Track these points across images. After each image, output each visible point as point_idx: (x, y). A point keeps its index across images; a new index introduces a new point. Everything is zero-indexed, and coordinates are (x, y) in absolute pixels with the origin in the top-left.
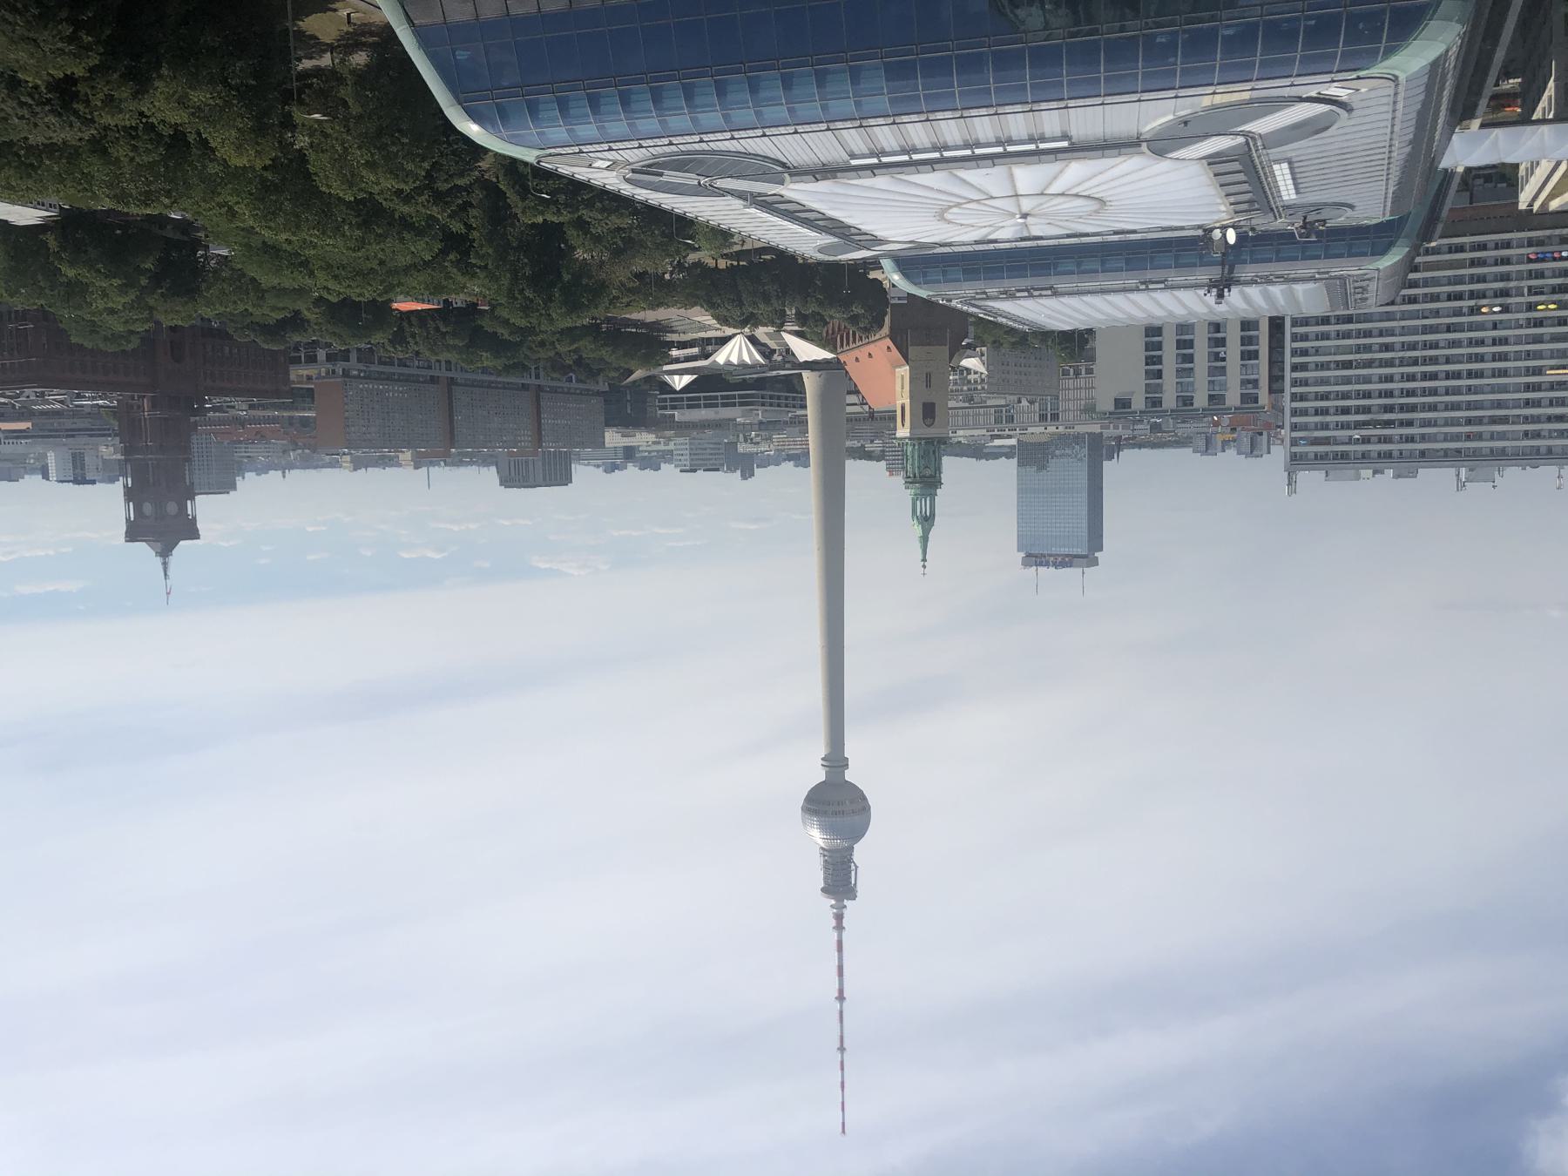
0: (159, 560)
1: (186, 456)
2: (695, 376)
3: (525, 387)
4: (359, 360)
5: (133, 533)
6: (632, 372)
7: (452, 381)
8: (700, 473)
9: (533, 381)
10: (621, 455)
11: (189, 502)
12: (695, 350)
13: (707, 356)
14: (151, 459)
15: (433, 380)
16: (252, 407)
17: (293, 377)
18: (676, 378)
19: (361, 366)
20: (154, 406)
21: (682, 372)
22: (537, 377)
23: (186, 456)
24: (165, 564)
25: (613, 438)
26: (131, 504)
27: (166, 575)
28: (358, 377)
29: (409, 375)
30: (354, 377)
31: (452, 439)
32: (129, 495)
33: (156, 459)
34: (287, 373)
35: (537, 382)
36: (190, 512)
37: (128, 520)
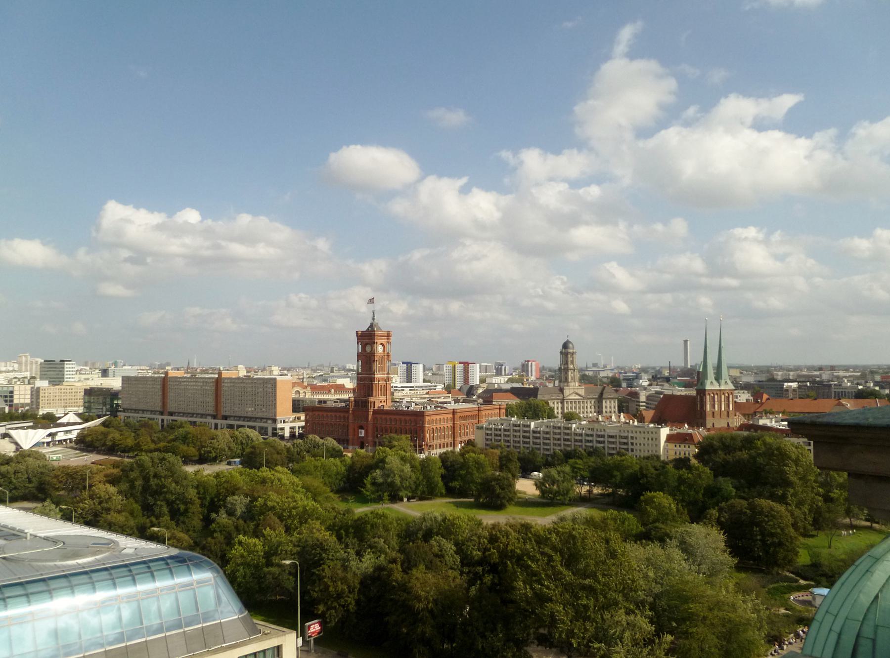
2: (58, 422)
3: (171, 414)
4: (266, 428)
5: (388, 336)
6: (104, 424)
7: (214, 417)
8: (58, 360)
9: (165, 417)
10: (111, 373)
11: (360, 351)
12: (58, 438)
13: (50, 435)
15: (225, 418)
16: (325, 402)
17: (303, 418)
18: (71, 421)
19: (265, 425)
20: (374, 403)
21: (69, 424)
22: (163, 420)
23: (360, 376)
24: (374, 319)
25: (115, 383)
29: (239, 420)
30: (269, 419)
31: (218, 382)
34: (306, 421)
35: (163, 417)
36: (360, 346)
37: (390, 343)
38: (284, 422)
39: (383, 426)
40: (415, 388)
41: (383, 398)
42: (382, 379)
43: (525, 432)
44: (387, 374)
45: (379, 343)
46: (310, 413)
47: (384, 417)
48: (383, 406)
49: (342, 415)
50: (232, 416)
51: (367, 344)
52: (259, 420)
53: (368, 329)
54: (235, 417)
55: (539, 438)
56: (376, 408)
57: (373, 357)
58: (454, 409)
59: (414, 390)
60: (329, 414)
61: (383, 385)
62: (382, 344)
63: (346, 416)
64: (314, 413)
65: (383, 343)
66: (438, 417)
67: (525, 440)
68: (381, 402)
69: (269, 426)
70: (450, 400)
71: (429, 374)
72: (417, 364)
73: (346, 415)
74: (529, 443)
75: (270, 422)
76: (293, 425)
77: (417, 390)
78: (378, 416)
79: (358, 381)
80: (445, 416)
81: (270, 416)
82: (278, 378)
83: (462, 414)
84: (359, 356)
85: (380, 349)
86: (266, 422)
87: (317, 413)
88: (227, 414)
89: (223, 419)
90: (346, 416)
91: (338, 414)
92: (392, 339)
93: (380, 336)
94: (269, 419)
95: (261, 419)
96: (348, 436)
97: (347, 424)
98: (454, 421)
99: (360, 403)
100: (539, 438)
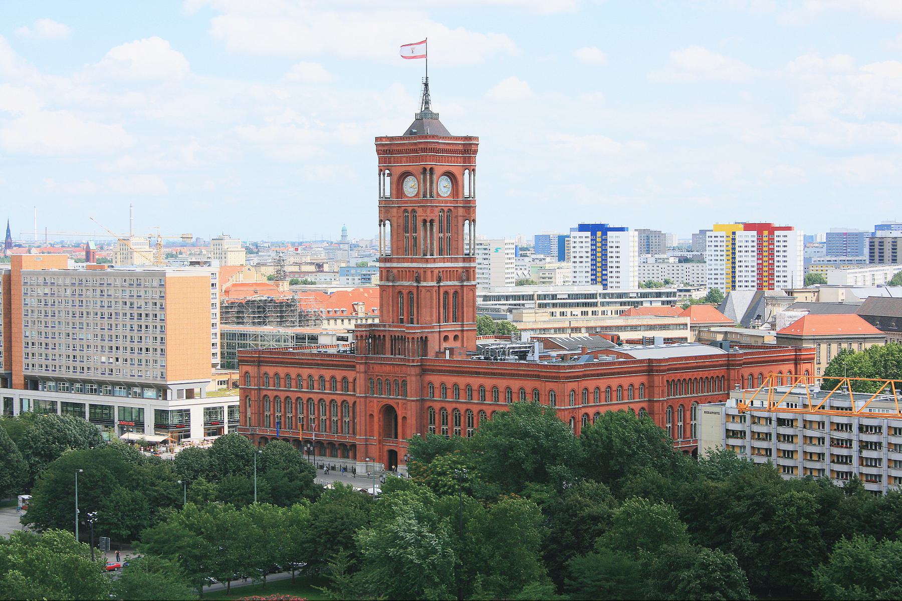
0: (433, 108)
1: (388, 265)
4: (141, 411)
11: (388, 194)
14: (434, 261)
15: (33, 383)
20: (424, 341)
23: (388, 265)
24: (427, 102)
26: (466, 193)
27: (426, 85)
28: (144, 386)
30: (149, 386)
32: (468, 208)
33: (427, 261)
36: (388, 179)
38: (190, 394)
39: (462, 408)
40: (599, 300)
41: (451, 327)
42: (450, 273)
43: (839, 427)
44: (464, 260)
45: (439, 170)
46: (252, 370)
47: (450, 380)
48: (452, 350)
49: (339, 374)
50: (48, 379)
51: (405, 175)
52: (123, 392)
53: (410, 132)
54: (58, 380)
55: (877, 445)
56: (431, 355)
57: (420, 212)
58: (650, 361)
59: (595, 304)
60: (305, 372)
61: (451, 292)
62: (450, 175)
63: (351, 380)
64: (264, 369)
65: (453, 169)
66: (603, 383)
67: (837, 451)
68: (446, 338)
69: (149, 404)
70: (687, 333)
71: (672, 260)
72: (621, 229)
73: (351, 376)
74: (847, 460)
75: (150, 393)
76: (213, 402)
77: (603, 304)
78: (436, 379)
79: (381, 280)
80: (625, 381)
81: (150, 375)
82: (171, 272)
83: (678, 376)
84: (385, 207)
85: (444, 187)
86: (141, 396)
87: (271, 370)
88: (37, 372)
89: (26, 388)
90: (351, 380)
91: (327, 374)
92: (481, 160)
93: (444, 151)
94: (149, 386)
95: (129, 386)
96: (354, 433)
97: (351, 401)
98: (651, 394)
99: (387, 339)
100: (877, 445)
